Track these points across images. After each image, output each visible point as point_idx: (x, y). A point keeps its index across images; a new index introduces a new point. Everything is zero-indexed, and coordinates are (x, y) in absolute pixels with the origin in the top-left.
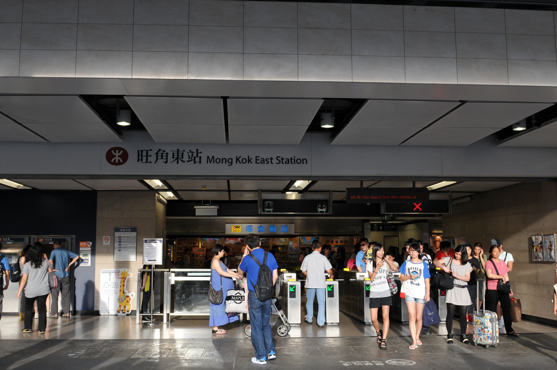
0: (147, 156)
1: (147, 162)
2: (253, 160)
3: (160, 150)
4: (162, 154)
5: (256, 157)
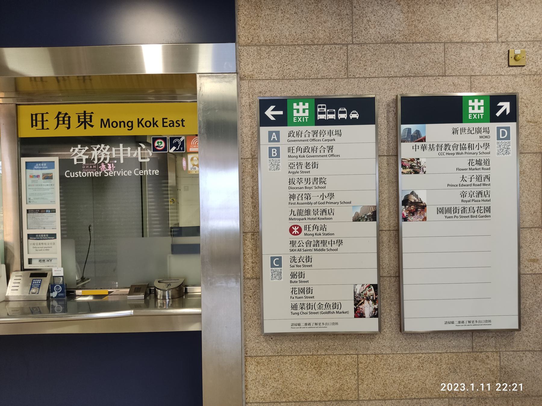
0: (43, 121)
1: (43, 128)
2: (160, 123)
3: (60, 113)
4: (64, 118)
5: (163, 119)
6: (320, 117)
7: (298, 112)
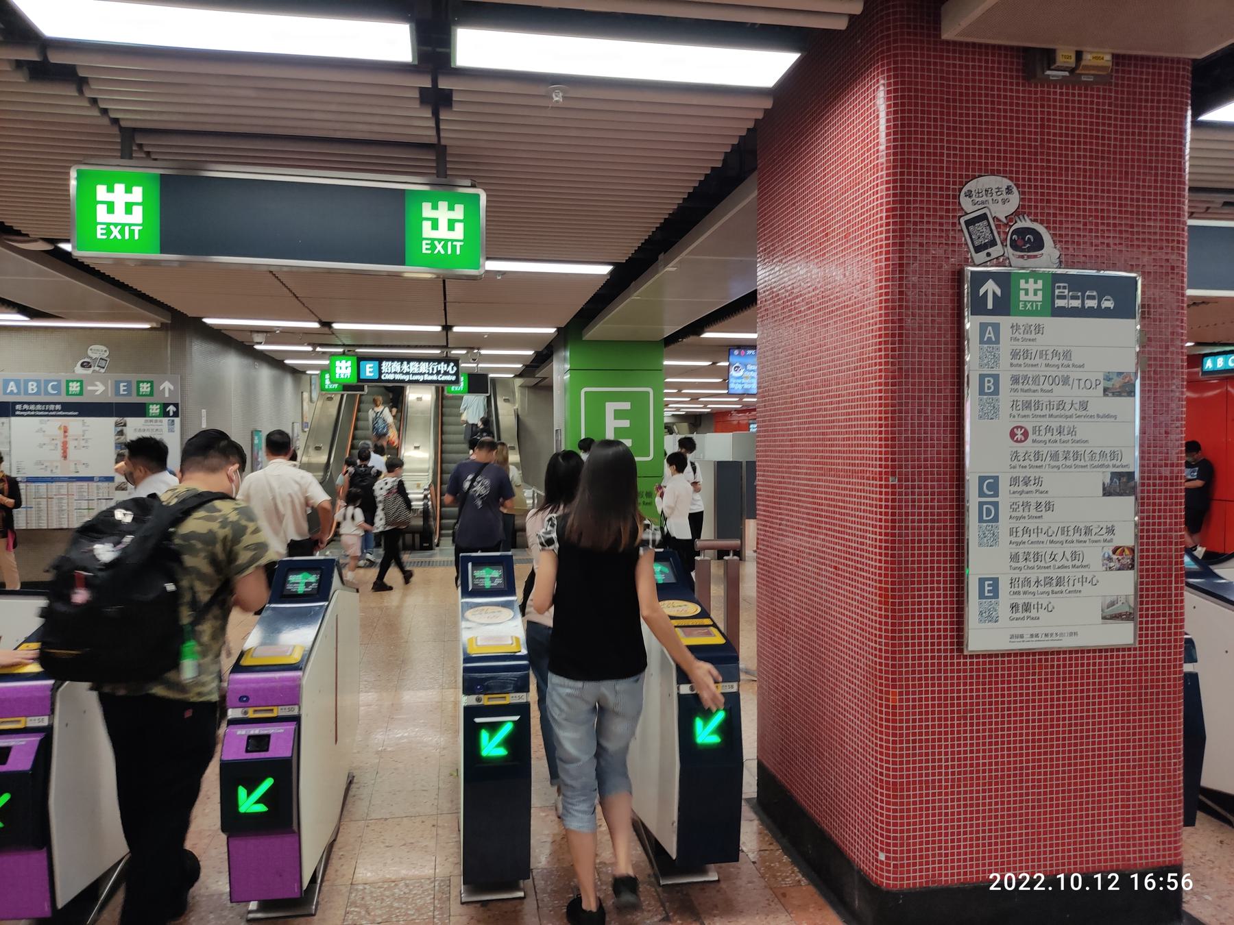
6: (1059, 303)
7: (1027, 294)
